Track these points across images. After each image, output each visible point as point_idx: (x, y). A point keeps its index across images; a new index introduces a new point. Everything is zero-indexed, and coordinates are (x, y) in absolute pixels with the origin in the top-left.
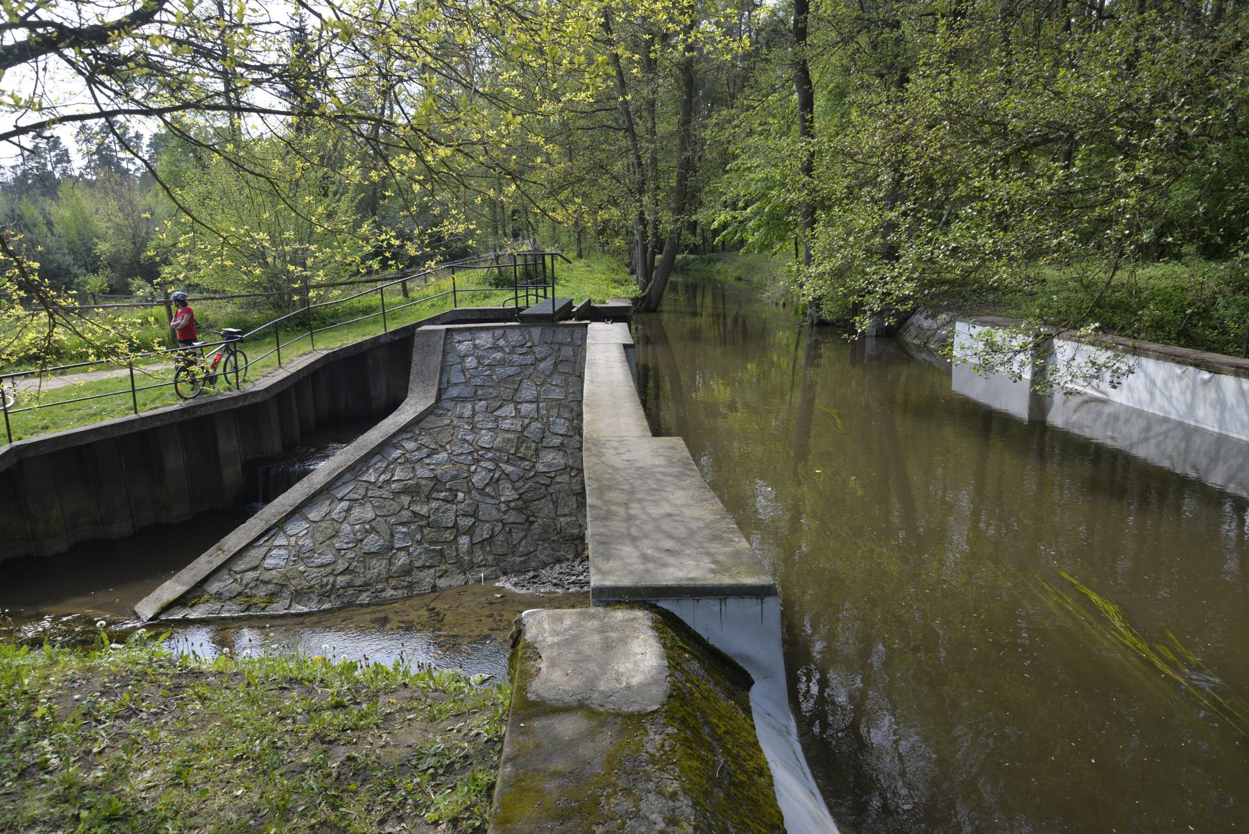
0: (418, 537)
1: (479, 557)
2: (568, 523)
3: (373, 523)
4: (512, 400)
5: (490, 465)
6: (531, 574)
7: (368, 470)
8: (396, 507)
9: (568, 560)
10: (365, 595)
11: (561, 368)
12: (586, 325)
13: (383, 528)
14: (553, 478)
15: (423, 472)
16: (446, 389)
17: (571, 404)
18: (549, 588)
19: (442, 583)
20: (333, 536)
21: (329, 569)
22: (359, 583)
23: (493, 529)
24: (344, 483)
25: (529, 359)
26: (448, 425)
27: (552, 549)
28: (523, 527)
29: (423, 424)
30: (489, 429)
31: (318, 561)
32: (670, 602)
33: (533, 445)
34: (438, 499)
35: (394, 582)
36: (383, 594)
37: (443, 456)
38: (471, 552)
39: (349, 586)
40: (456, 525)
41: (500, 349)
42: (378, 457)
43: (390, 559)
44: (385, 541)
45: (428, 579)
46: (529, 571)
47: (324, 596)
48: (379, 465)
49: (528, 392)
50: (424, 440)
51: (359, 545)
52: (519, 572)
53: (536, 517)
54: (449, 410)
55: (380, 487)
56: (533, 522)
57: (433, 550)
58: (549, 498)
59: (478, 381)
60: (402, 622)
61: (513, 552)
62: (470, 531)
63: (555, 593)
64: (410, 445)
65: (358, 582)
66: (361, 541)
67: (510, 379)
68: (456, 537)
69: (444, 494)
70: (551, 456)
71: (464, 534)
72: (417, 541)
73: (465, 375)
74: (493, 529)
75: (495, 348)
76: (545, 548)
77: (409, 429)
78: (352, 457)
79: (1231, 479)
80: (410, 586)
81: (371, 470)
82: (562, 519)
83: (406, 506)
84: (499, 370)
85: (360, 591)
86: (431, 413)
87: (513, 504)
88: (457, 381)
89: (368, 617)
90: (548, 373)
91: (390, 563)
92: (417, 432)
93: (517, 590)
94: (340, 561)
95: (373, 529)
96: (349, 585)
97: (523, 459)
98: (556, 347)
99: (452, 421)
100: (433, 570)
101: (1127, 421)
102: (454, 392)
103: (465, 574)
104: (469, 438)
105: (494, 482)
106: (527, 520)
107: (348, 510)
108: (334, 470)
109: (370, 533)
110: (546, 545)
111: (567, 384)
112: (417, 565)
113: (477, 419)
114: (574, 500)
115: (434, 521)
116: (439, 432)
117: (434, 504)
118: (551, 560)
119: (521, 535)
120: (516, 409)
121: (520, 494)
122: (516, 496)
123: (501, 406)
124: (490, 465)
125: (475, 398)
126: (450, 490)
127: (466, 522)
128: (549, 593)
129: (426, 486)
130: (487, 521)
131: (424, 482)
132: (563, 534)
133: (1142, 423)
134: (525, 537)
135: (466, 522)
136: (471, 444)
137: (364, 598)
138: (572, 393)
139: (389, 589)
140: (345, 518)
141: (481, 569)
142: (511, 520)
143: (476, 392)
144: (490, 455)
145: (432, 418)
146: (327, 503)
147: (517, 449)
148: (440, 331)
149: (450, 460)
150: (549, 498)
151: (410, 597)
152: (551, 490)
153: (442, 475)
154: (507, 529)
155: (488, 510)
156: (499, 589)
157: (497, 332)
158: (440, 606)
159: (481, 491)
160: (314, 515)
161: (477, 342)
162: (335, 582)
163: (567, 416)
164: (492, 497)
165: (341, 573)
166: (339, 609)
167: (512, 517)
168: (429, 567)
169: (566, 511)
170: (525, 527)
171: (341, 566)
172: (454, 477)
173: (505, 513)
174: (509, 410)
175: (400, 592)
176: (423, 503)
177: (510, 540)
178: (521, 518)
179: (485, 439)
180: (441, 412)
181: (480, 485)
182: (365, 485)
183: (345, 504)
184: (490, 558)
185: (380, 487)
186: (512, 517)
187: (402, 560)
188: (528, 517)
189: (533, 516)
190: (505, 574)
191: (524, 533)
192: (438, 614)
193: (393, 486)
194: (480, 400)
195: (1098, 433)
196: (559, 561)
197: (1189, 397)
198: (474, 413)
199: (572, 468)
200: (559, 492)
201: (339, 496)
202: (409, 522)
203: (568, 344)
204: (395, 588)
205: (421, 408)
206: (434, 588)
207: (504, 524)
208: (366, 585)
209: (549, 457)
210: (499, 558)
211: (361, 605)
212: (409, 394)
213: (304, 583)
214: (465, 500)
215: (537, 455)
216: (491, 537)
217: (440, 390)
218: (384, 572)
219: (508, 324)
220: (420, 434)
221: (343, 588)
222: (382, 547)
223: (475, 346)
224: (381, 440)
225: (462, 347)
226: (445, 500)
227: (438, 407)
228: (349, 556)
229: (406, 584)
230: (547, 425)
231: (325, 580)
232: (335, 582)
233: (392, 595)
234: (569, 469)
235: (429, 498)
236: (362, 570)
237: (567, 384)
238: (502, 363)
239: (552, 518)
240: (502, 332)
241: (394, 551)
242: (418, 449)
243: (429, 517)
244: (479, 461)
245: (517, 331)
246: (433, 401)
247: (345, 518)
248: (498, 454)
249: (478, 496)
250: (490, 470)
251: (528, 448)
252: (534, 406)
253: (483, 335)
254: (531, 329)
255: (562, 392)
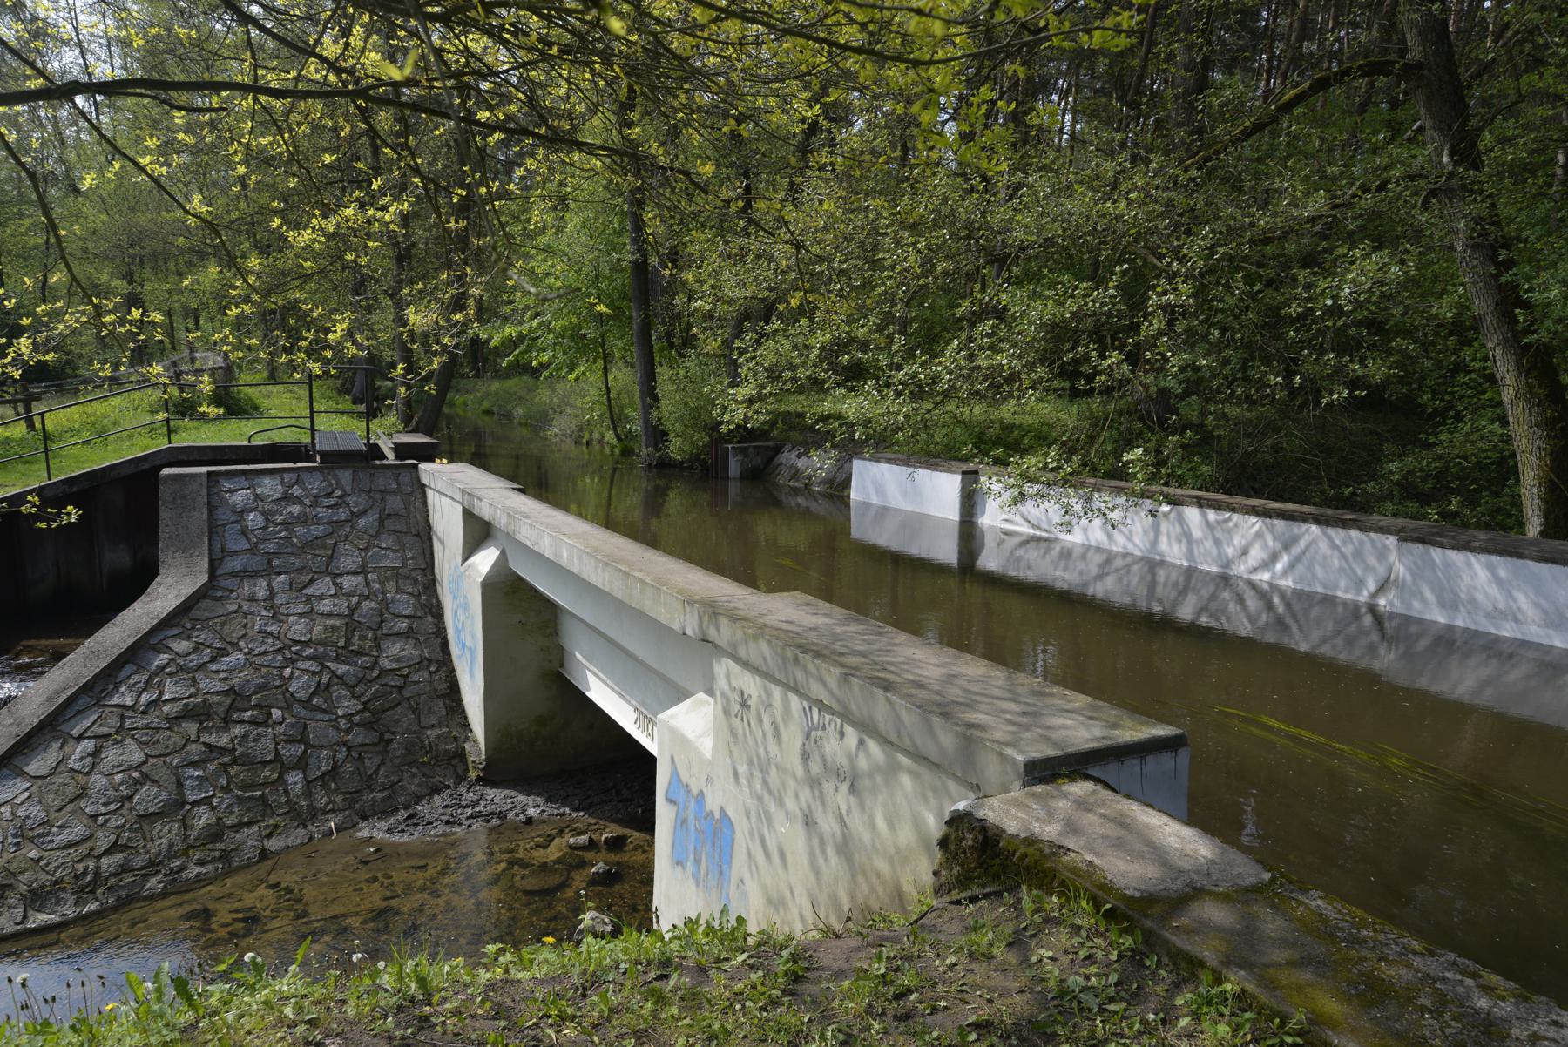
0: (223, 781)
1: (321, 799)
2: (438, 737)
3: (144, 769)
4: (327, 572)
5: (312, 666)
6: (402, 814)
7: (117, 688)
8: (176, 739)
9: (448, 787)
10: (153, 880)
11: (390, 524)
12: (415, 467)
13: (162, 774)
14: (407, 676)
15: (209, 684)
16: (222, 559)
17: (414, 574)
18: (441, 828)
19: (274, 844)
20: (79, 797)
21: (83, 849)
22: (141, 864)
23: (334, 757)
24: (79, 712)
25: (342, 513)
26: (236, 612)
27: (424, 775)
28: (377, 749)
29: (194, 613)
30: (301, 615)
31: (60, 839)
32: (1098, 768)
33: (370, 634)
34: (243, 722)
35: (197, 855)
36: (184, 875)
37: (236, 657)
38: (308, 794)
39: (124, 871)
40: (278, 757)
41: (297, 500)
42: (129, 668)
43: (183, 820)
44: (170, 793)
45: (250, 842)
46: (397, 810)
47: (84, 891)
48: (134, 678)
49: (348, 560)
50: (202, 636)
51: (127, 805)
52: (385, 813)
53: (393, 733)
54: (232, 591)
55: (144, 713)
56: (389, 741)
57: (249, 797)
58: (405, 704)
59: (271, 547)
60: (237, 911)
61: (369, 787)
62: (301, 764)
63: (452, 834)
64: (182, 646)
65: (138, 862)
66: (130, 798)
67: (319, 541)
68: (281, 775)
69: (250, 713)
70: (398, 646)
71: (293, 768)
72: (222, 788)
73: (248, 539)
74: (334, 757)
75: (288, 499)
76: (414, 776)
77: (175, 622)
78: (85, 672)
79: (1202, 610)
80: (225, 856)
81: (123, 689)
82: (429, 732)
83: (193, 737)
84: (300, 530)
85: (144, 875)
86: (205, 596)
87: (357, 718)
88: (236, 548)
89: (172, 913)
90: (372, 532)
91: (185, 827)
92: (188, 625)
93: (396, 838)
94: (100, 834)
95: (146, 778)
96: (124, 869)
97: (359, 653)
98: (378, 496)
99: (240, 606)
100: (255, 828)
101: (1083, 557)
102: (236, 564)
103: (305, 827)
104: (273, 628)
105: (322, 690)
106: (381, 739)
107: (96, 753)
108: (58, 693)
109: (143, 784)
110: (414, 770)
111: (403, 546)
112: (229, 823)
113: (278, 601)
114: (441, 704)
115: (242, 754)
116: (223, 624)
117: (238, 730)
118: (425, 791)
119: (377, 761)
120: (335, 584)
121: (364, 703)
122: (360, 707)
123: (311, 581)
124: (314, 667)
125: (269, 571)
126: (258, 706)
127: (292, 751)
128: (444, 835)
129: (219, 704)
130: (324, 747)
131: (214, 699)
132: (435, 753)
133: (1098, 559)
134: (382, 763)
135: (292, 751)
136: (277, 638)
137: (154, 884)
138: (412, 558)
139: (191, 865)
140: (94, 765)
141: (329, 816)
142: (359, 740)
143: (269, 562)
144: (309, 651)
145: (206, 603)
146: (57, 745)
147: (348, 641)
148: (200, 475)
149: (248, 663)
150: (405, 704)
151: (226, 874)
152: (406, 693)
153: (242, 686)
154: (355, 754)
155: (319, 729)
156: (369, 840)
157: (287, 477)
158: (288, 878)
159: (306, 704)
160: (35, 767)
161: (259, 490)
162: (97, 869)
163: (410, 590)
164: (325, 712)
165: (107, 853)
166: (114, 909)
167: (358, 737)
168: (249, 824)
169: (433, 720)
170: (380, 748)
171: (103, 843)
172: (261, 688)
173: (348, 731)
174: (324, 585)
175: (210, 867)
176: (218, 730)
177: (362, 769)
178: (372, 737)
179: (297, 629)
180: (219, 594)
181: (303, 696)
182: (118, 711)
183: (88, 745)
184: (338, 798)
185: (144, 713)
186: (358, 737)
187: (203, 819)
188: (382, 734)
189: (388, 732)
190: (365, 818)
191: (380, 758)
192: (289, 891)
193: (166, 709)
194: (279, 574)
195: (1063, 577)
196: (436, 790)
197: (1152, 535)
198: (272, 594)
199: (430, 661)
200: (419, 695)
201: (75, 732)
202: (204, 761)
203: (394, 492)
204: (201, 863)
205: (187, 588)
206: (264, 855)
207: (349, 749)
208: (153, 866)
209: (395, 648)
210: (352, 798)
211: (152, 898)
212: (162, 570)
213: (43, 877)
214: (284, 719)
215: (378, 647)
216: (333, 768)
217: (211, 562)
218: (178, 841)
219: (299, 465)
220: (193, 628)
221: (114, 875)
222: (166, 803)
223: (257, 496)
224: (131, 641)
225: (239, 498)
226: (253, 722)
227: (213, 587)
228: (112, 823)
229: (217, 854)
230: (385, 603)
231: (80, 867)
232: (98, 867)
233: (199, 874)
234: (426, 663)
235: (227, 723)
236: (142, 843)
237: (403, 546)
238: (303, 520)
239: (415, 733)
240: (295, 476)
241: (188, 807)
242: (195, 650)
243: (234, 749)
244: (293, 661)
245: (317, 475)
246: (205, 578)
247: (94, 765)
248: (321, 649)
249: (304, 712)
250: (314, 673)
251: (363, 638)
252: (360, 578)
253: (267, 480)
254: (337, 472)
255: (397, 558)
